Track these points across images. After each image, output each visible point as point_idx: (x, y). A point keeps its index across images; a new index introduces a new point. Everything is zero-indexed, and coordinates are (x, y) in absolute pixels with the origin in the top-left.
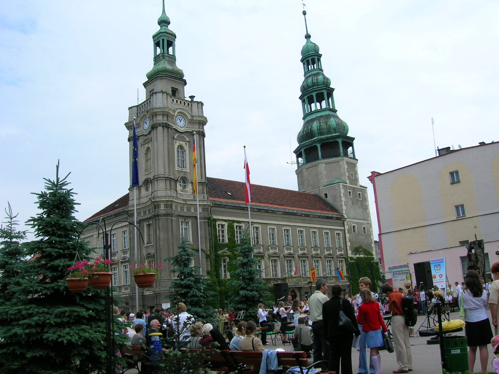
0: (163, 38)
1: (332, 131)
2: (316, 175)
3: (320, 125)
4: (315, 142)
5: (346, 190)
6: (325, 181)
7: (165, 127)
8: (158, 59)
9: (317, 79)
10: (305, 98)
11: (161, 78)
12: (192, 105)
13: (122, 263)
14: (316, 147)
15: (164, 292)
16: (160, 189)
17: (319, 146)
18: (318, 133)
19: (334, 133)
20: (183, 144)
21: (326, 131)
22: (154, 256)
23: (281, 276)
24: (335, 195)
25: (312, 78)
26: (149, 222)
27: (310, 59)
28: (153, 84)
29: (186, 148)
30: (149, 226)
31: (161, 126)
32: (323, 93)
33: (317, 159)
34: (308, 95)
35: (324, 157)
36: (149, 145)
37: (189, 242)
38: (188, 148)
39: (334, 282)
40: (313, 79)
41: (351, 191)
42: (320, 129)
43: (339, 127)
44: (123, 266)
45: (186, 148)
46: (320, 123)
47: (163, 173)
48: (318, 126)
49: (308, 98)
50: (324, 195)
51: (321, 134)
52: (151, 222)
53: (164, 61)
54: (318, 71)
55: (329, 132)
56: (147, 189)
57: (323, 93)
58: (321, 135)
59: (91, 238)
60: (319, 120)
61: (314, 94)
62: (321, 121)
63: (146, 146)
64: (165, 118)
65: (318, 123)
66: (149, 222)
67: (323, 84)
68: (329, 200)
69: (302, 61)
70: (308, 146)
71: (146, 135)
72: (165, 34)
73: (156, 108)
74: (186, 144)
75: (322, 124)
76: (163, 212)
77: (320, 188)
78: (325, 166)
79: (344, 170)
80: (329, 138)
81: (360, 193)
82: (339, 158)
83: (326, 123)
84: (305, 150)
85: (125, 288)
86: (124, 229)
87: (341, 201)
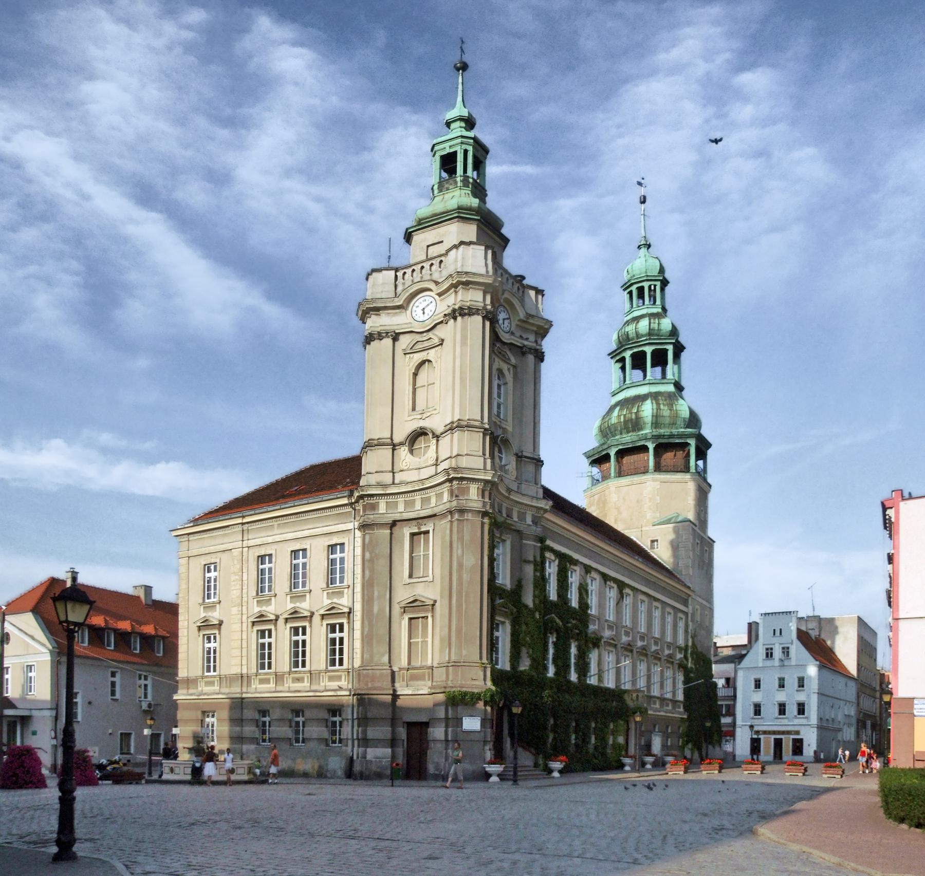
1: (679, 423)
2: (638, 502)
3: (658, 409)
20: (505, 367)
21: (667, 421)
26: (419, 528)
27: (634, 288)
29: (509, 377)
38: (512, 380)
42: (656, 416)
45: (509, 377)
46: (658, 404)
48: (655, 411)
57: (666, 351)
59: (224, 556)
61: (649, 350)
62: (661, 402)
66: (419, 528)
74: (509, 369)
75: (662, 407)
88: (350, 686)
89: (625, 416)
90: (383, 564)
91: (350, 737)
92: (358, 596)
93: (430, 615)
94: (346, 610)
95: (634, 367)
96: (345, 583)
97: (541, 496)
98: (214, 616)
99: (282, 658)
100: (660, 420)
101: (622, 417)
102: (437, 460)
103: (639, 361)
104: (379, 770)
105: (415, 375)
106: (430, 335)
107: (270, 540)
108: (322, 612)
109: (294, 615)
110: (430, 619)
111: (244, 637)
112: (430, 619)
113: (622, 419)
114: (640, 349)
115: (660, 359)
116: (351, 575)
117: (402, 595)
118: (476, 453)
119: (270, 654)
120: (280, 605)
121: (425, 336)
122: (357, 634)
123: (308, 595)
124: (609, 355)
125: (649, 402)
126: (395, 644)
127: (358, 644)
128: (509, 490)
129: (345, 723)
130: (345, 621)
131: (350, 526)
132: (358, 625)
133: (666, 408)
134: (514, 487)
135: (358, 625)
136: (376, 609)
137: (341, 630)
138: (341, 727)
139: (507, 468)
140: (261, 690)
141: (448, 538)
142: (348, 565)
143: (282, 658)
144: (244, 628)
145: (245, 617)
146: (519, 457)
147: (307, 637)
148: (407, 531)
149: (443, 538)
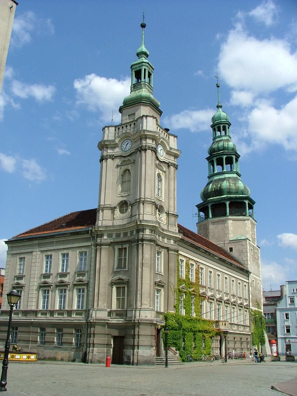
0: (146, 68)
5: (250, 248)
6: (232, 237)
7: (154, 151)
8: (139, 87)
9: (228, 145)
10: (215, 159)
11: (145, 104)
12: (169, 137)
14: (225, 205)
15: (144, 321)
16: (146, 213)
17: (228, 203)
18: (227, 192)
19: (241, 195)
23: (214, 319)
24: (241, 250)
25: (224, 142)
26: (122, 246)
28: (136, 107)
29: (163, 177)
30: (120, 250)
31: (150, 149)
32: (232, 157)
33: (225, 214)
34: (218, 157)
35: (231, 214)
36: (129, 167)
37: (161, 272)
38: (164, 178)
39: (242, 330)
40: (225, 143)
41: (252, 248)
43: (245, 190)
44: (42, 290)
46: (229, 183)
47: (150, 198)
50: (229, 249)
51: (229, 193)
52: (127, 246)
53: (146, 89)
54: (228, 138)
55: (237, 193)
58: (229, 194)
60: (229, 181)
61: (224, 157)
62: (231, 182)
63: (123, 168)
64: (154, 143)
65: (228, 183)
66: (122, 246)
67: (232, 150)
68: (234, 254)
70: (216, 201)
71: (125, 157)
72: (147, 64)
73: (148, 131)
75: (231, 184)
76: (148, 237)
77: (225, 242)
78: (232, 222)
79: (249, 229)
80: (233, 198)
81: (257, 252)
82: (245, 218)
83: (235, 184)
84: (211, 206)
85: (42, 313)
86: (83, 250)
87: (247, 256)
91: (85, 342)
93: (126, 286)
94: (86, 282)
97: (178, 232)
98: (22, 282)
100: (231, 190)
101: (213, 189)
102: (131, 216)
103: (220, 163)
104: (99, 359)
106: (129, 158)
107: (51, 248)
110: (126, 288)
112: (126, 288)
113: (213, 190)
115: (229, 161)
118: (148, 213)
121: (127, 159)
124: (206, 159)
125: (225, 182)
128: (163, 230)
129: (83, 335)
130: (85, 287)
131: (89, 244)
133: (233, 185)
134: (165, 228)
139: (162, 219)
146: (168, 214)
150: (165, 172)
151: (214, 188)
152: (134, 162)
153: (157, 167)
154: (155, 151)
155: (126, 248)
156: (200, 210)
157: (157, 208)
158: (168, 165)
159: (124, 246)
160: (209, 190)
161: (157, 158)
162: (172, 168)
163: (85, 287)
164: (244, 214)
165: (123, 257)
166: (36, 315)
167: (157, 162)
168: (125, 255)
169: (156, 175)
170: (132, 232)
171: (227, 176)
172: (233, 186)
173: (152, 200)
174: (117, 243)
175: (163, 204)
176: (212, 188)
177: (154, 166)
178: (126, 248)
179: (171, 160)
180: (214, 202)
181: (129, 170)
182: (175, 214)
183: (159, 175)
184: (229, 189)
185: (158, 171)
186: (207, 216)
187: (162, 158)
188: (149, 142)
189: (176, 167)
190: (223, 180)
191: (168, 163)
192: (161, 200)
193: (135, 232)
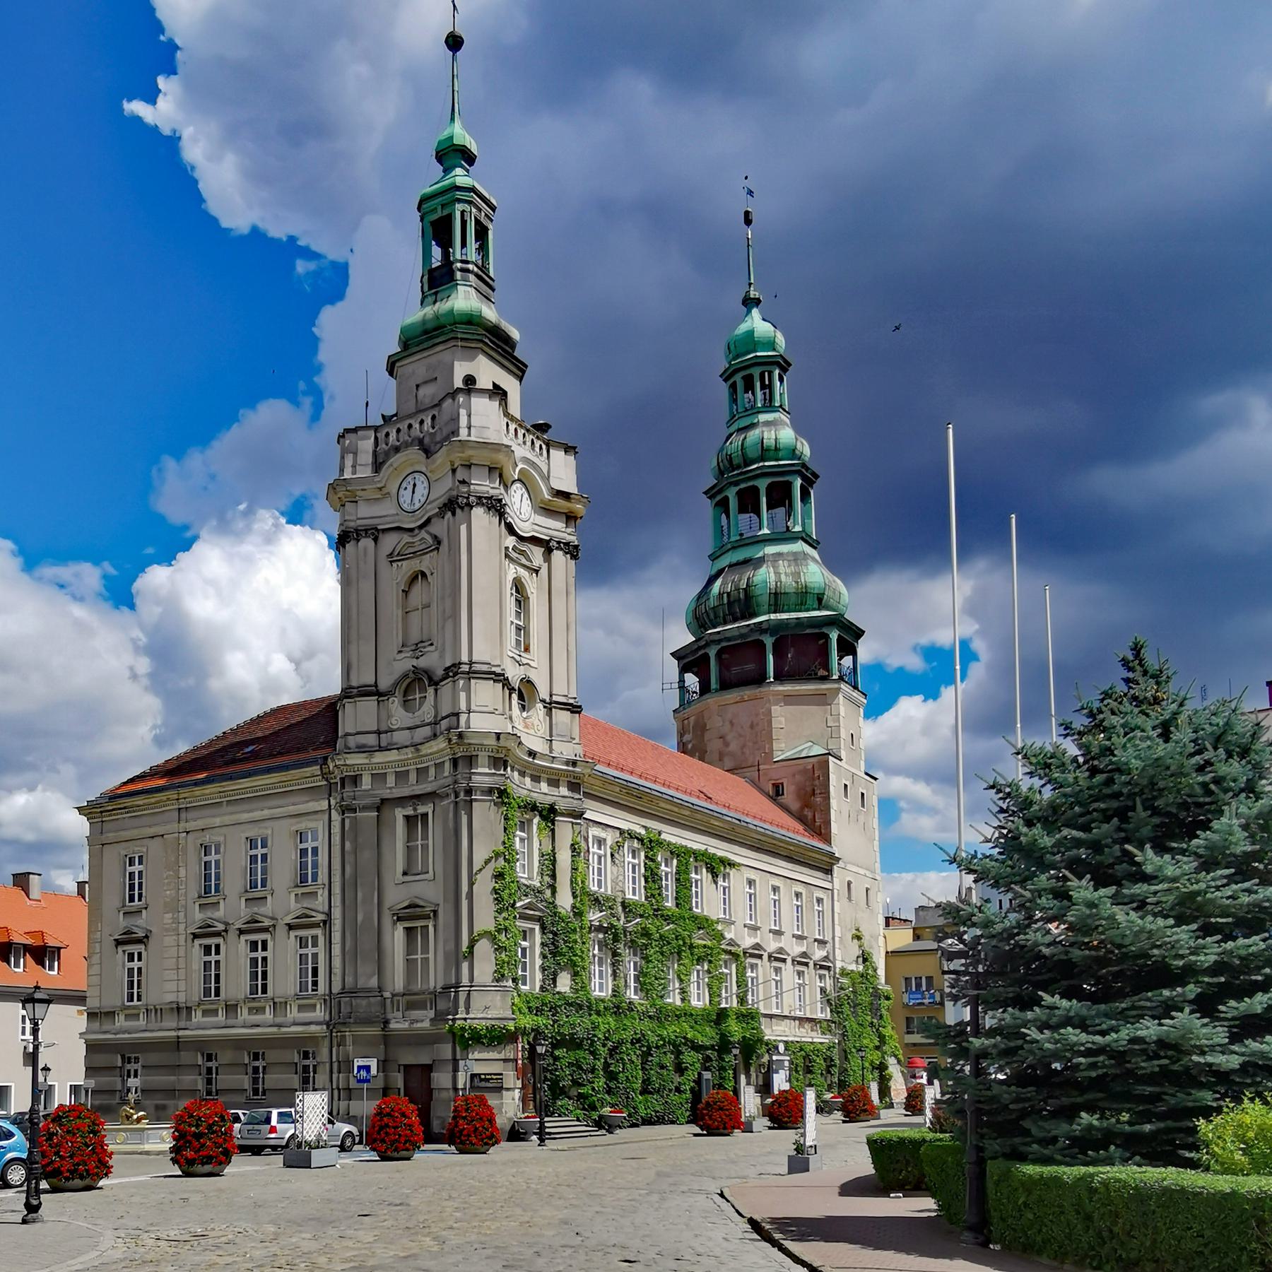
4: (759, 628)
13: (291, 927)
14: (761, 646)
19: (814, 609)
22: (435, 912)
26: (415, 809)
29: (533, 587)
36: (425, 564)
46: (777, 574)
49: (740, 494)
52: (427, 808)
56: (406, 704)
57: (789, 485)
61: (762, 484)
62: (782, 570)
63: (408, 567)
65: (772, 575)
66: (415, 809)
69: (727, 376)
75: (783, 577)
86: (303, 825)
88: (327, 1018)
89: (729, 594)
90: (367, 856)
92: (337, 900)
94: (321, 917)
95: (742, 509)
96: (320, 881)
98: (140, 924)
99: (236, 983)
102: (436, 716)
105: (406, 592)
108: (288, 920)
109: (252, 926)
111: (182, 953)
114: (750, 484)
116: (326, 870)
117: (396, 896)
119: (217, 976)
120: (233, 909)
122: (336, 949)
123: (269, 898)
125: (763, 570)
126: (388, 963)
127: (337, 963)
132: (337, 937)
135: (337, 937)
136: (360, 918)
137: (315, 945)
138: (315, 1072)
140: (203, 1026)
141: (451, 824)
142: (323, 858)
143: (236, 983)
144: (182, 942)
145: (182, 927)
147: (268, 954)
148: (399, 814)
149: (445, 821)
150: (537, 572)
151: (729, 594)
152: (438, 549)
153: (511, 560)
154: (497, 507)
155: (425, 815)
156: (683, 670)
157: (512, 690)
158: (547, 546)
159: (422, 809)
160: (712, 602)
161: (511, 530)
162: (558, 556)
163: (318, 932)
164: (822, 672)
165: (419, 842)
166: (189, 1018)
167: (511, 541)
168: (425, 837)
169: (509, 585)
170: (439, 766)
171: (770, 550)
172: (788, 582)
173: (494, 669)
174: (401, 801)
175: (533, 676)
176: (720, 595)
177: (499, 556)
178: (425, 815)
179: (555, 528)
180: (728, 639)
181: (424, 575)
182: (571, 701)
183: (518, 586)
184: (776, 594)
185: (512, 571)
186: (705, 688)
187: (525, 529)
188: (483, 485)
189: (572, 551)
190: (762, 560)
191: (548, 542)
192: (525, 661)
193: (447, 765)
